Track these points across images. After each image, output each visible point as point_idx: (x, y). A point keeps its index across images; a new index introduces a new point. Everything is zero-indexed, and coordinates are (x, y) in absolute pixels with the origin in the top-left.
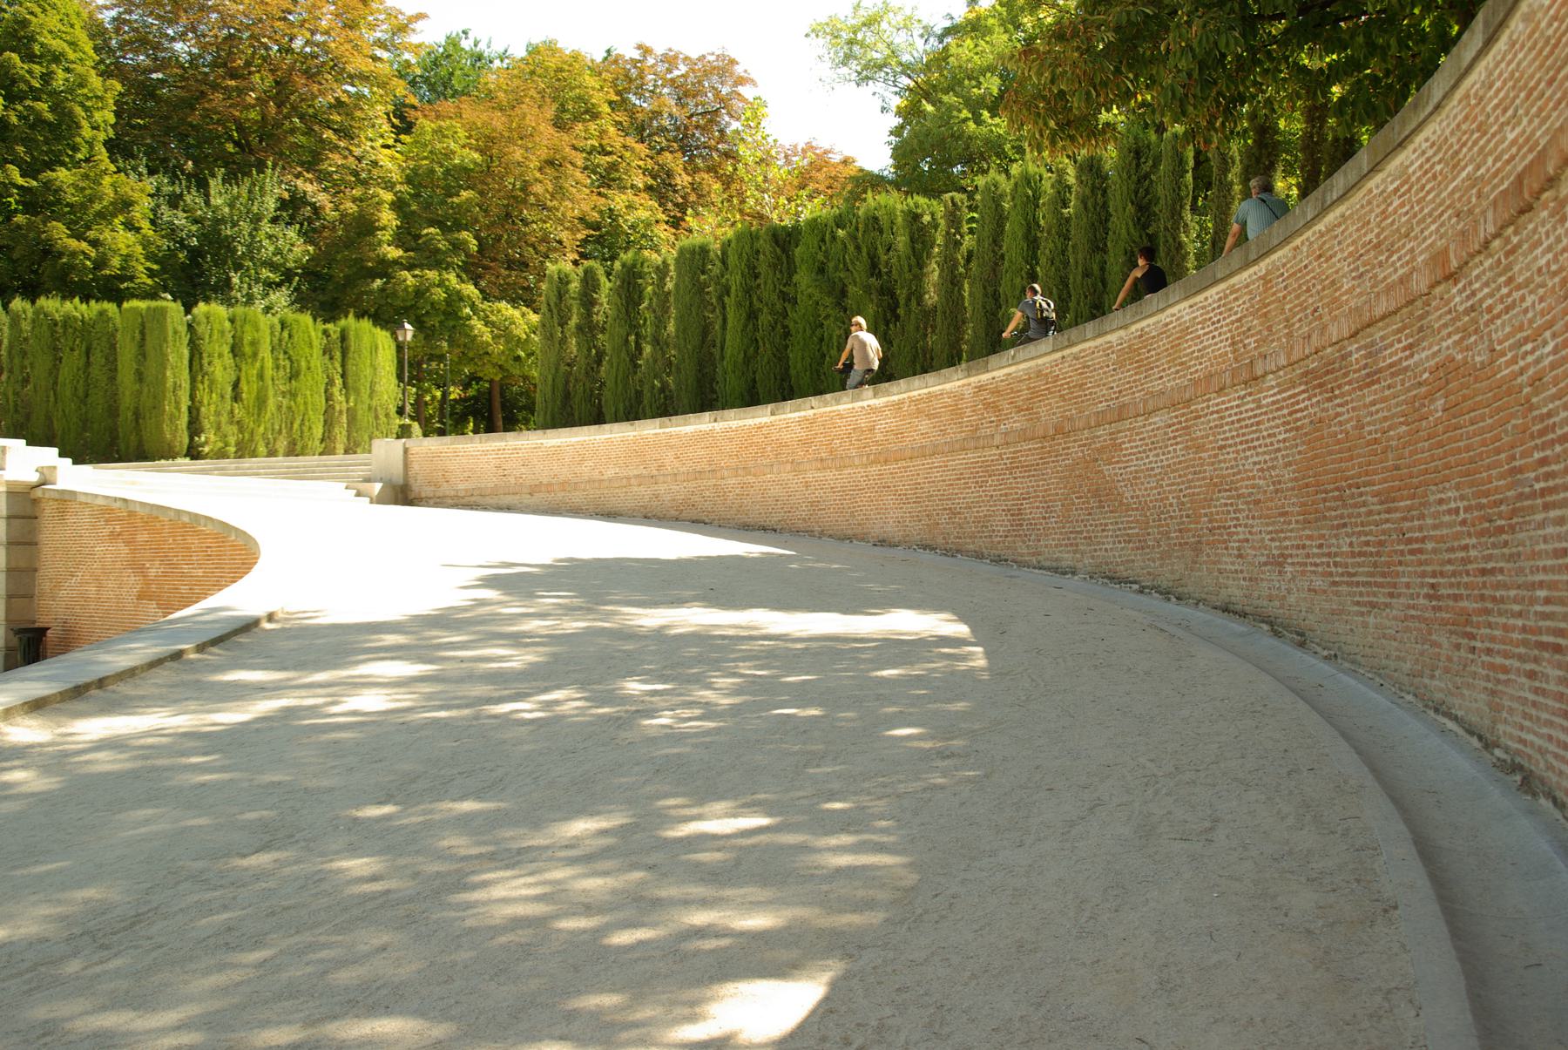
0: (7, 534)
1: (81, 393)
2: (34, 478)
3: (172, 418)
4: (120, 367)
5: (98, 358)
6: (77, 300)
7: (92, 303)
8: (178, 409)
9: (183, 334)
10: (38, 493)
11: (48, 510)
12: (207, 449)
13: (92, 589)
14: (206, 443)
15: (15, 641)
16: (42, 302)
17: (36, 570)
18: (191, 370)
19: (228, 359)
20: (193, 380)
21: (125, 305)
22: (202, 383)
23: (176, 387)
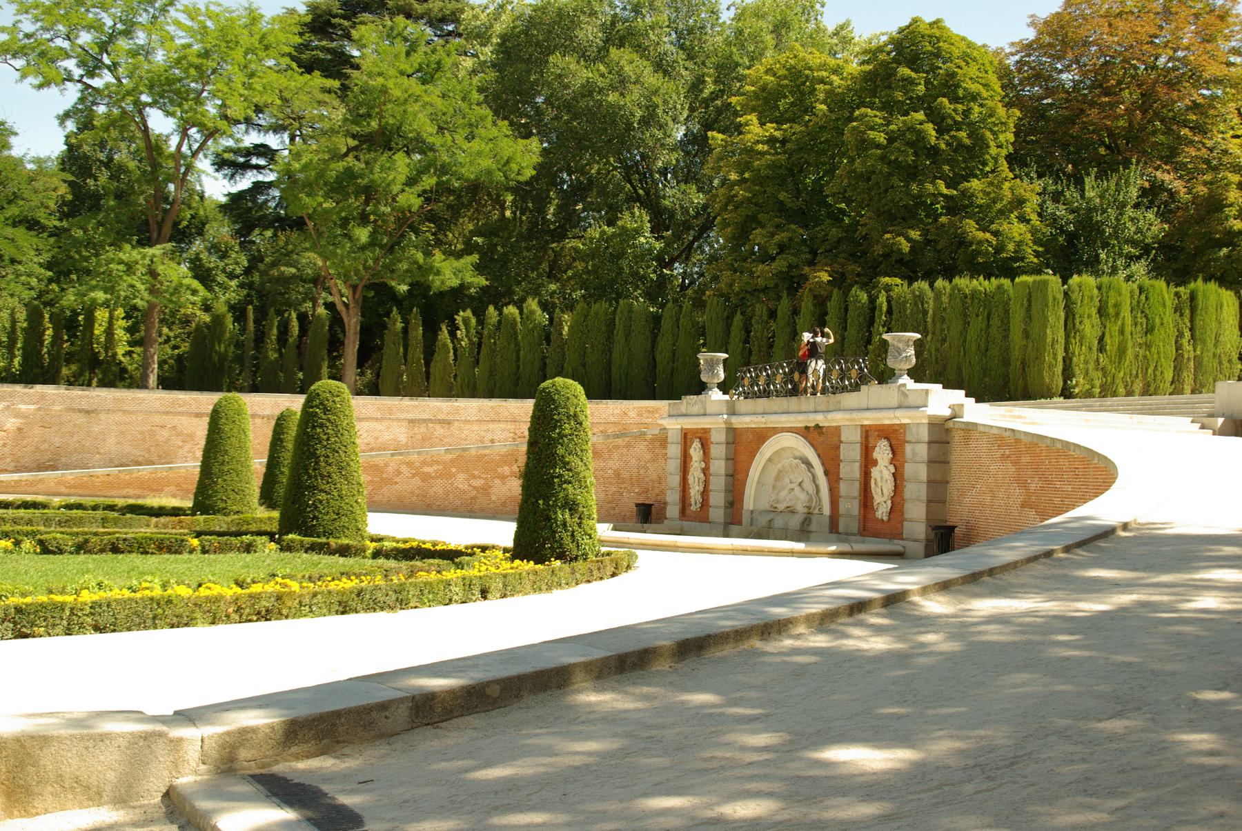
0: (928, 454)
1: (983, 348)
2: (947, 413)
3: (1051, 366)
4: (1011, 328)
5: (995, 321)
6: (981, 277)
7: (993, 279)
8: (1055, 359)
9: (1061, 300)
10: (950, 424)
11: (957, 437)
12: (1077, 390)
13: (988, 499)
14: (1077, 385)
15: (932, 536)
16: (957, 280)
17: (948, 482)
18: (1065, 329)
19: (1096, 319)
20: (1067, 337)
21: (1017, 280)
22: (1075, 338)
23: (1054, 342)
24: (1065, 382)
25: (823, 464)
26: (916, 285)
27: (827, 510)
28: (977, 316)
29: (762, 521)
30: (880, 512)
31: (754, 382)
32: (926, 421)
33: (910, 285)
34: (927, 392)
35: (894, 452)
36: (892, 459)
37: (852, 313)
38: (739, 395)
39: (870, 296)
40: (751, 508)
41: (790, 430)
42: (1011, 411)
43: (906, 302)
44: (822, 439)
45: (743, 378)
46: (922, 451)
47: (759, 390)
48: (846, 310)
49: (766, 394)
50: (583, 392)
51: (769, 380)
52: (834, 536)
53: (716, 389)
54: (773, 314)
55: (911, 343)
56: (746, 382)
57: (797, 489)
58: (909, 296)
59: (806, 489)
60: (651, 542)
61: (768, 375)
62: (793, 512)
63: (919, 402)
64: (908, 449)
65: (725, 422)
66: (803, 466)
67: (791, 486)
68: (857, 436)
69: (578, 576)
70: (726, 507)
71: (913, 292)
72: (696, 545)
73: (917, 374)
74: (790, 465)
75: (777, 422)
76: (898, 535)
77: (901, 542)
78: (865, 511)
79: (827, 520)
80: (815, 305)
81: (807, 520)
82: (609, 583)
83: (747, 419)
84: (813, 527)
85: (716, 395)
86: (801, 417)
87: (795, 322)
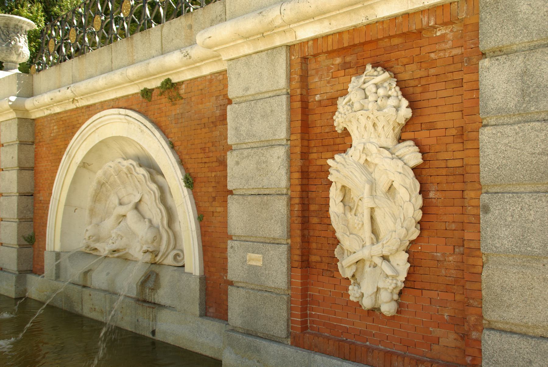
25: (182, 163)
40: (57, 249)
41: (115, 104)
44: (178, 109)
57: (132, 216)
59: (148, 215)
65: (14, 107)
66: (142, 171)
67: (121, 210)
70: (21, 246)
74: (118, 172)
78: (305, 277)
79: (195, 286)
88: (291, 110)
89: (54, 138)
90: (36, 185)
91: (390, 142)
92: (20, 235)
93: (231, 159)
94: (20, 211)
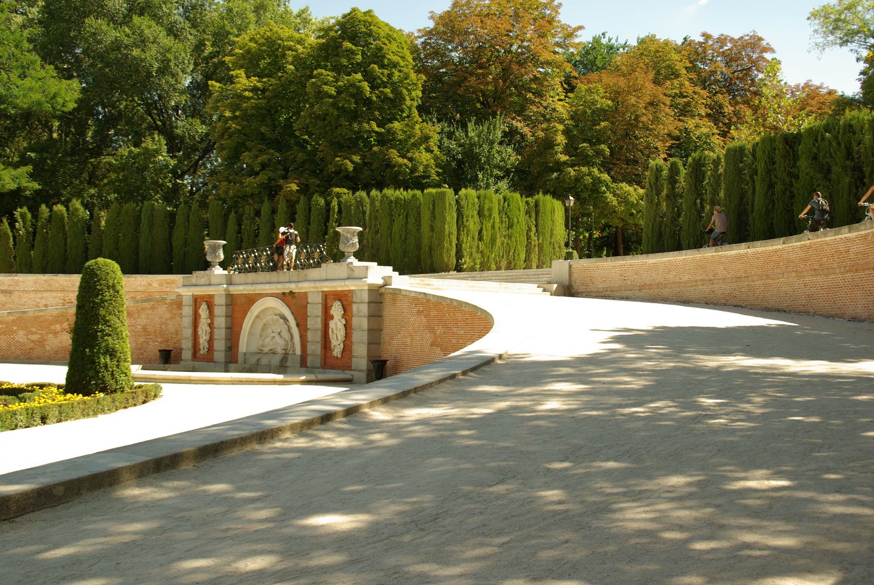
2: (381, 282)
3: (448, 250)
5: (412, 219)
6: (402, 189)
7: (409, 190)
8: (451, 245)
10: (383, 290)
11: (388, 299)
12: (465, 266)
13: (409, 341)
14: (465, 263)
15: (371, 367)
17: (382, 330)
20: (458, 230)
22: (463, 231)
23: (450, 233)
24: (457, 261)
25: (295, 319)
26: (358, 194)
27: (298, 351)
28: (399, 215)
29: (253, 360)
30: (336, 352)
31: (246, 261)
32: (366, 288)
33: (354, 193)
34: (367, 268)
35: (345, 310)
36: (344, 315)
37: (314, 213)
38: (235, 270)
39: (326, 201)
40: (244, 351)
41: (271, 295)
42: (423, 281)
43: (351, 205)
44: (294, 301)
45: (237, 259)
46: (364, 309)
47: (249, 267)
48: (310, 210)
49: (254, 269)
50: (119, 269)
51: (257, 260)
52: (304, 369)
53: (218, 266)
54: (258, 213)
55: (356, 234)
56: (240, 261)
57: (277, 338)
58: (353, 201)
59: (284, 337)
60: (171, 378)
61: (255, 256)
62: (274, 353)
63: (361, 275)
64: (355, 307)
65: (225, 290)
66: (282, 320)
67: (274, 335)
68: (319, 299)
69: (118, 404)
70: (226, 351)
71: (356, 199)
72: (205, 379)
73: (360, 256)
74: (272, 320)
75: (262, 290)
76: (348, 367)
77: (350, 372)
79: (299, 358)
80: (288, 207)
81: (285, 358)
82: (140, 408)
83: (241, 288)
84: (289, 363)
85: (218, 271)
86: (279, 286)
87: (273, 219)
88: (322, 308)
89: (243, 304)
90: (232, 324)
91: (340, 318)
92: (226, 346)
93: (309, 319)
94: (226, 335)
